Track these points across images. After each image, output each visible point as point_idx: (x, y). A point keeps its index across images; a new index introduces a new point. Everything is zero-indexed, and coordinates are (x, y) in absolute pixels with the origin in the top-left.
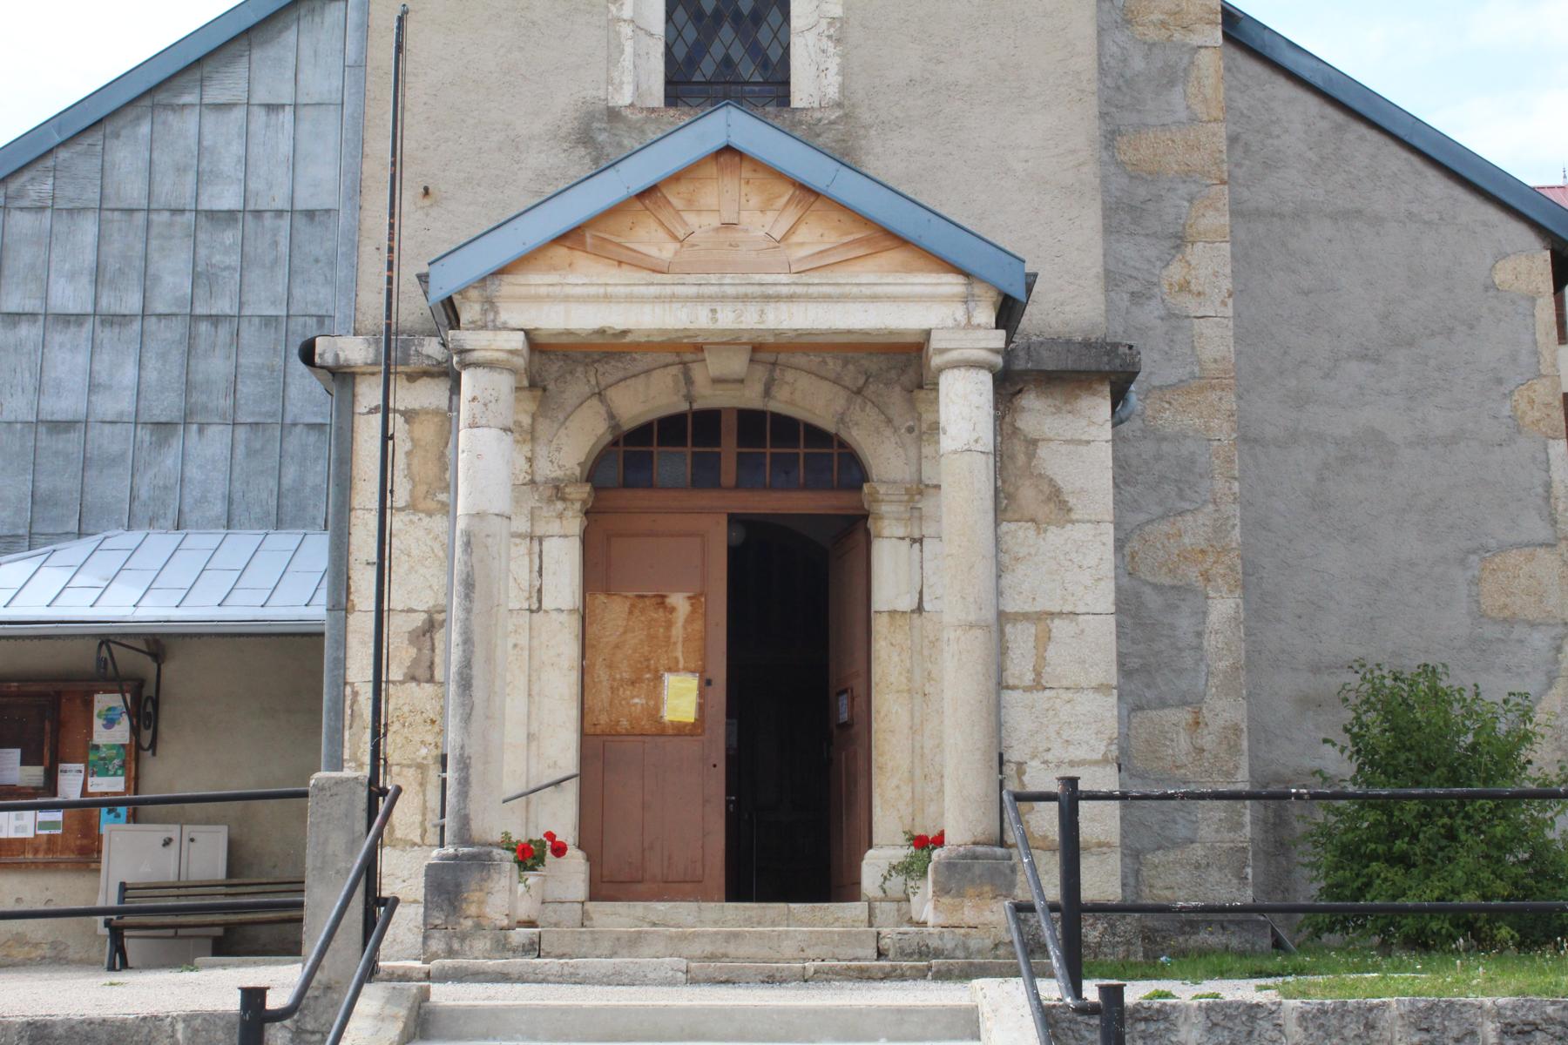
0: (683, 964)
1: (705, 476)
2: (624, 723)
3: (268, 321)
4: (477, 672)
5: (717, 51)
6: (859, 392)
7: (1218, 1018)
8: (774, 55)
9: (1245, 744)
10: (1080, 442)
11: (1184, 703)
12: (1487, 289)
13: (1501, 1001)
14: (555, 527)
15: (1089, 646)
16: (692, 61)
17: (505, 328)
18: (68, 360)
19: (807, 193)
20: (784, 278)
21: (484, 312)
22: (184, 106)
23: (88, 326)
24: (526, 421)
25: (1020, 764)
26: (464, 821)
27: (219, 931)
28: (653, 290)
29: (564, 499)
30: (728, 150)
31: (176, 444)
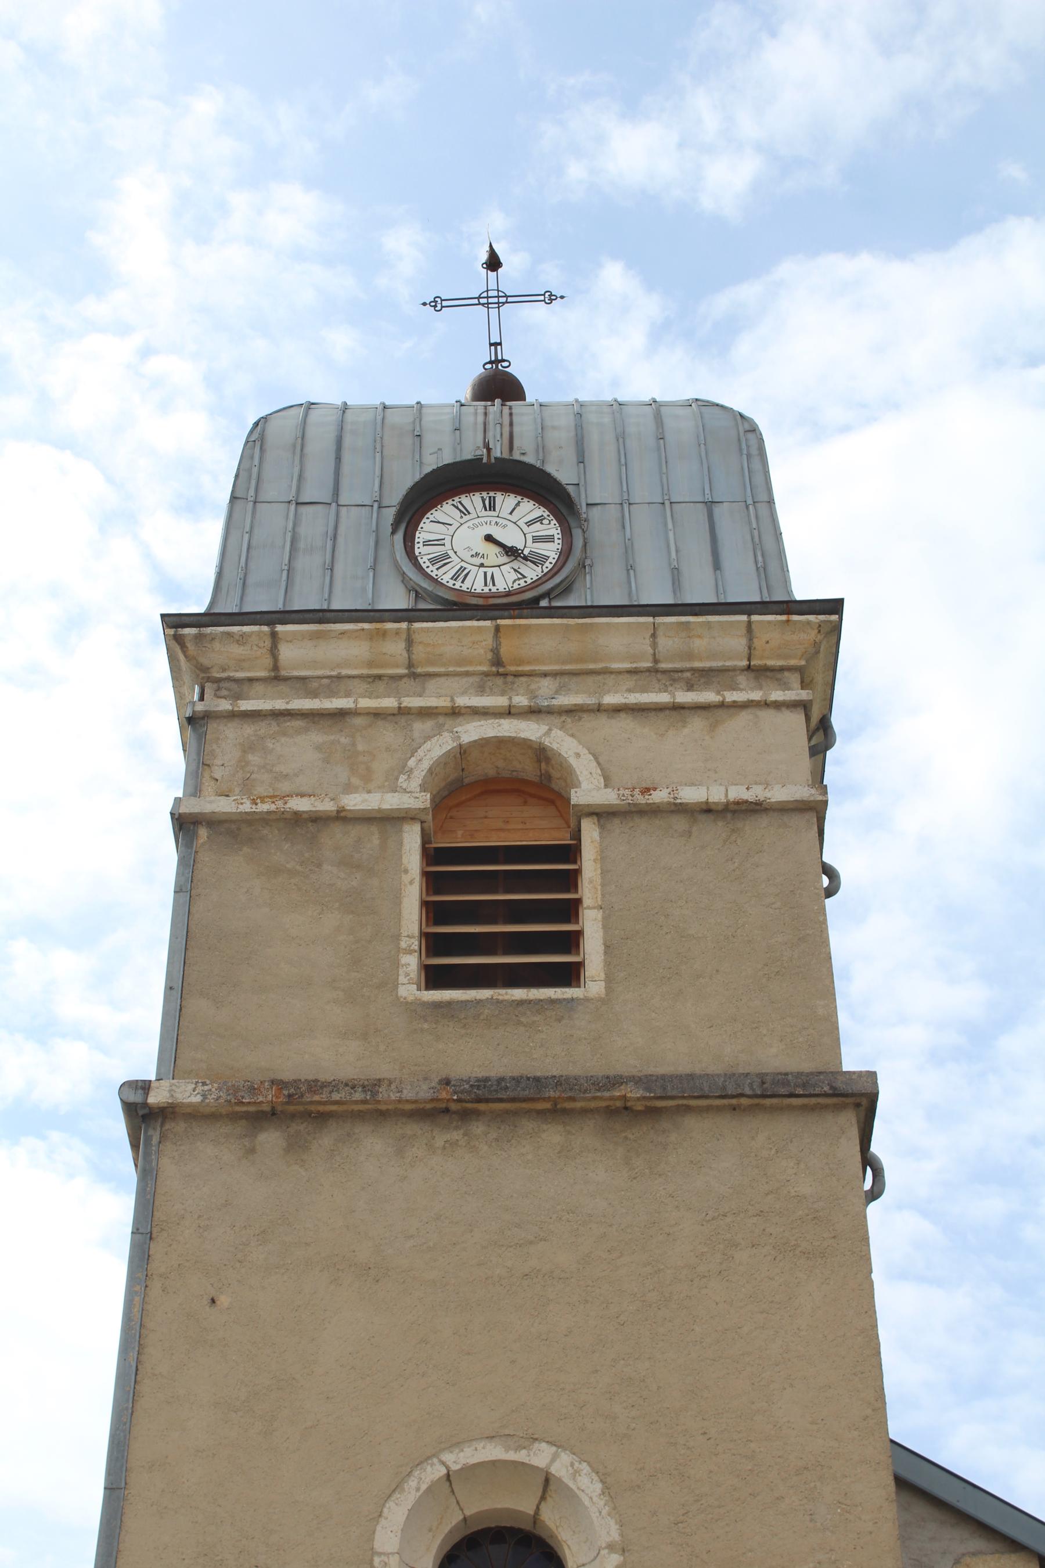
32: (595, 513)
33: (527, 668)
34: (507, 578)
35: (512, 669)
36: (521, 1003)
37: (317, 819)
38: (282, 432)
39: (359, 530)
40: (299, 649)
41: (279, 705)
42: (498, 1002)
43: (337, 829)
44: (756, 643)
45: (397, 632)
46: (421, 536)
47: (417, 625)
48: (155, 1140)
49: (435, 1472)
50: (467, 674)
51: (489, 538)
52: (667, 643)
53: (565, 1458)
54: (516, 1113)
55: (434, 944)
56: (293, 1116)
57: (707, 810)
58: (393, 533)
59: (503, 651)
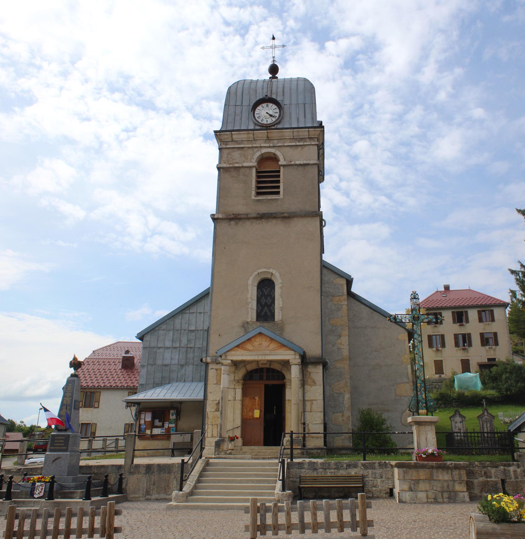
1: (261, 378)
3: (199, 348)
5: (264, 311)
11: (341, 412)
14: (238, 387)
15: (319, 405)
18: (168, 354)
19: (272, 340)
25: (308, 424)
30: (260, 333)
31: (184, 368)
34: (270, 121)
36: (270, 199)
37: (239, 167)
38: (233, 91)
39: (246, 109)
41: (233, 146)
43: (242, 169)
46: (256, 112)
51: (267, 113)
53: (274, 271)
55: (258, 188)
57: (300, 165)
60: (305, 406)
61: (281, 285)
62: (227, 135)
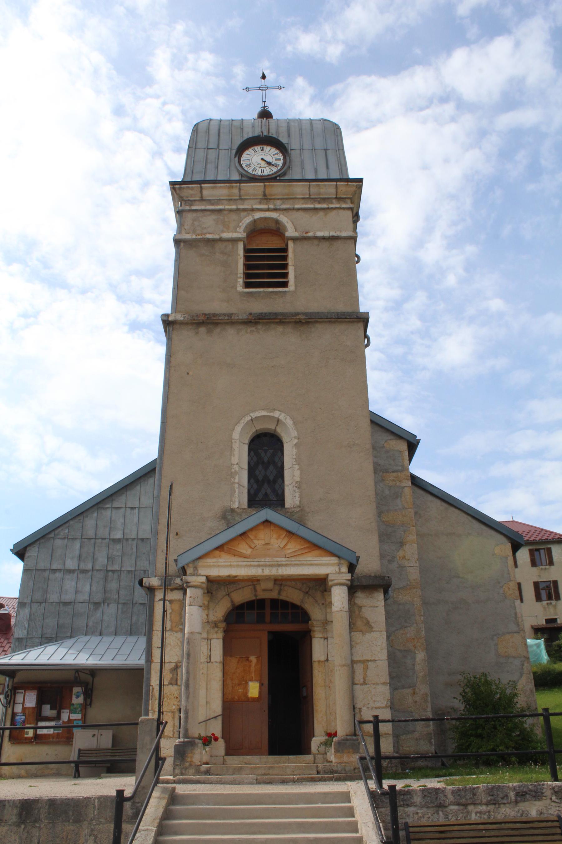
0: (255, 777)
1: (261, 620)
2: (236, 698)
3: (129, 572)
4: (191, 682)
5: (263, 491)
6: (307, 593)
7: (426, 793)
8: (280, 492)
9: (429, 700)
10: (374, 607)
11: (410, 687)
12: (493, 555)
13: (515, 784)
14: (215, 636)
15: (379, 670)
16: (256, 494)
17: (200, 575)
18: (70, 584)
19: (290, 534)
20: (284, 559)
21: (194, 571)
22: (107, 508)
23: (76, 573)
24: (206, 603)
25: (360, 709)
26: (186, 731)
27: (109, 765)
28: (245, 563)
29: (217, 627)
31: (101, 609)
32: (293, 152)
33: (273, 197)
34: (267, 171)
35: (269, 197)
36: (271, 292)
37: (214, 240)
38: (202, 128)
39: (225, 157)
40: (208, 192)
42: (265, 292)
44: (339, 191)
45: (236, 187)
46: (243, 159)
47: (242, 184)
48: (171, 329)
49: (248, 418)
50: (256, 199)
51: (262, 159)
52: (313, 190)
53: (283, 415)
54: (270, 323)
55: (247, 276)
56: (209, 323)
57: (324, 238)
58: (235, 157)
59: (267, 192)
60: (350, 673)
61: (296, 441)
62: (192, 189)
